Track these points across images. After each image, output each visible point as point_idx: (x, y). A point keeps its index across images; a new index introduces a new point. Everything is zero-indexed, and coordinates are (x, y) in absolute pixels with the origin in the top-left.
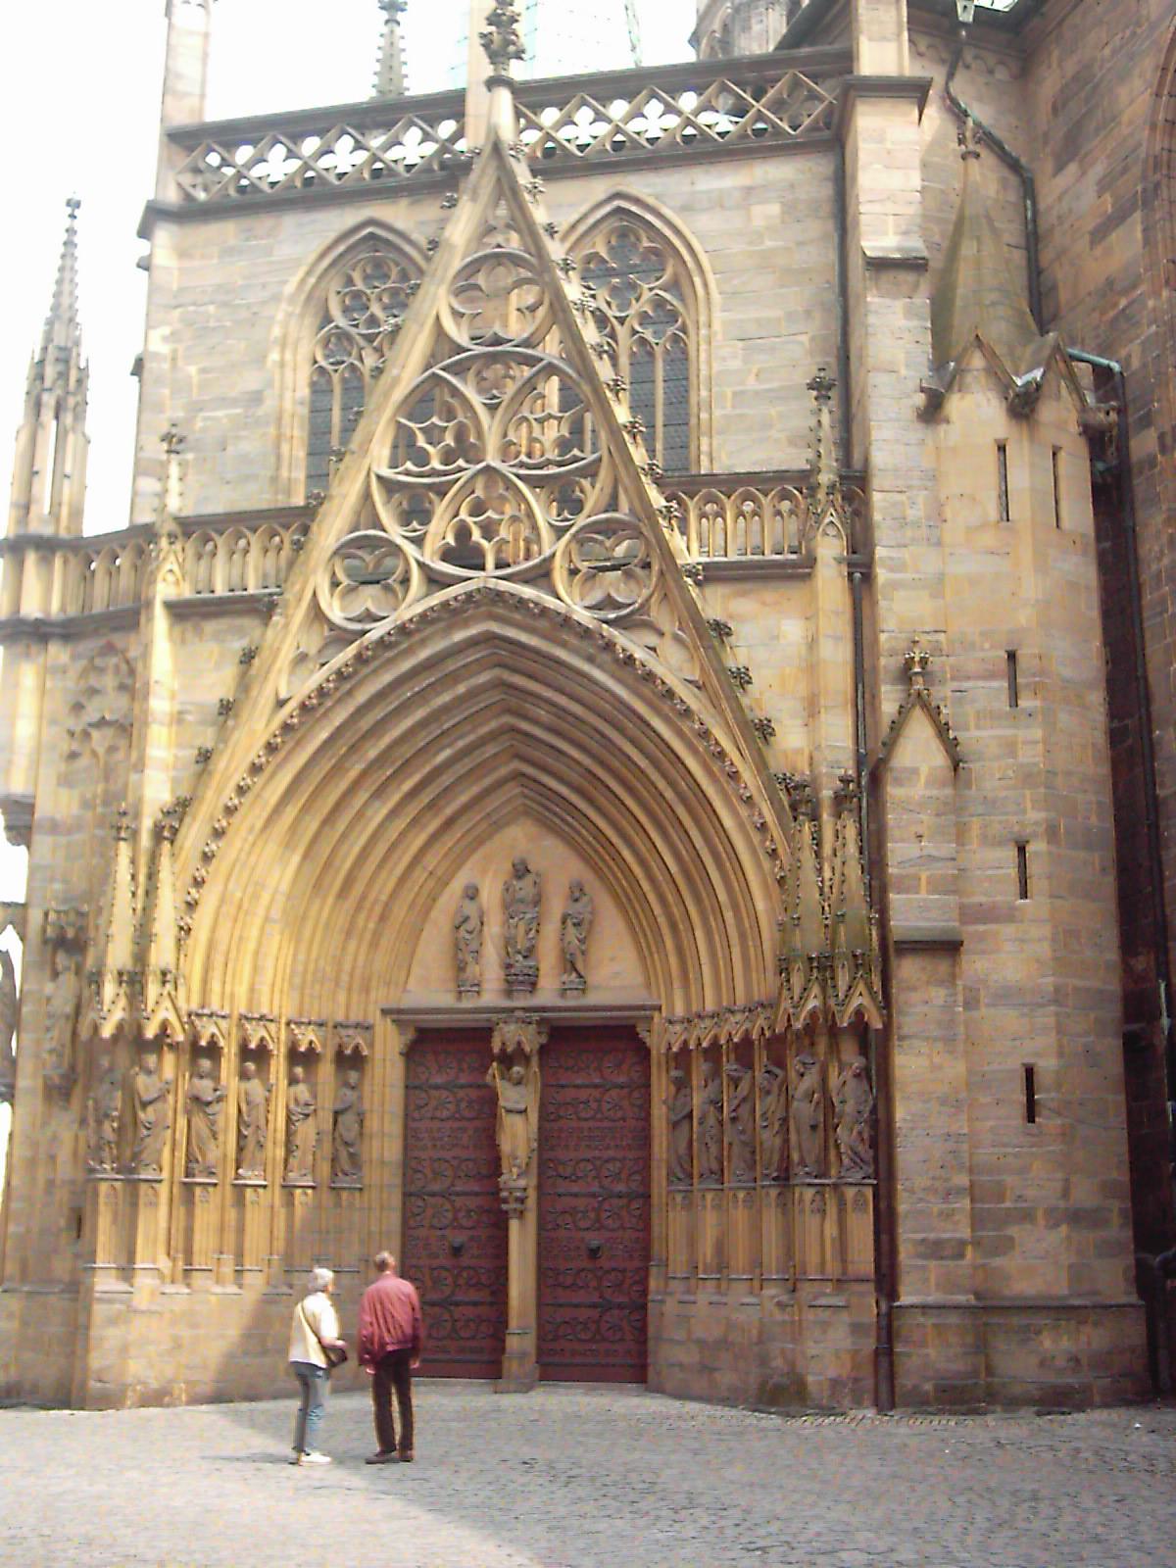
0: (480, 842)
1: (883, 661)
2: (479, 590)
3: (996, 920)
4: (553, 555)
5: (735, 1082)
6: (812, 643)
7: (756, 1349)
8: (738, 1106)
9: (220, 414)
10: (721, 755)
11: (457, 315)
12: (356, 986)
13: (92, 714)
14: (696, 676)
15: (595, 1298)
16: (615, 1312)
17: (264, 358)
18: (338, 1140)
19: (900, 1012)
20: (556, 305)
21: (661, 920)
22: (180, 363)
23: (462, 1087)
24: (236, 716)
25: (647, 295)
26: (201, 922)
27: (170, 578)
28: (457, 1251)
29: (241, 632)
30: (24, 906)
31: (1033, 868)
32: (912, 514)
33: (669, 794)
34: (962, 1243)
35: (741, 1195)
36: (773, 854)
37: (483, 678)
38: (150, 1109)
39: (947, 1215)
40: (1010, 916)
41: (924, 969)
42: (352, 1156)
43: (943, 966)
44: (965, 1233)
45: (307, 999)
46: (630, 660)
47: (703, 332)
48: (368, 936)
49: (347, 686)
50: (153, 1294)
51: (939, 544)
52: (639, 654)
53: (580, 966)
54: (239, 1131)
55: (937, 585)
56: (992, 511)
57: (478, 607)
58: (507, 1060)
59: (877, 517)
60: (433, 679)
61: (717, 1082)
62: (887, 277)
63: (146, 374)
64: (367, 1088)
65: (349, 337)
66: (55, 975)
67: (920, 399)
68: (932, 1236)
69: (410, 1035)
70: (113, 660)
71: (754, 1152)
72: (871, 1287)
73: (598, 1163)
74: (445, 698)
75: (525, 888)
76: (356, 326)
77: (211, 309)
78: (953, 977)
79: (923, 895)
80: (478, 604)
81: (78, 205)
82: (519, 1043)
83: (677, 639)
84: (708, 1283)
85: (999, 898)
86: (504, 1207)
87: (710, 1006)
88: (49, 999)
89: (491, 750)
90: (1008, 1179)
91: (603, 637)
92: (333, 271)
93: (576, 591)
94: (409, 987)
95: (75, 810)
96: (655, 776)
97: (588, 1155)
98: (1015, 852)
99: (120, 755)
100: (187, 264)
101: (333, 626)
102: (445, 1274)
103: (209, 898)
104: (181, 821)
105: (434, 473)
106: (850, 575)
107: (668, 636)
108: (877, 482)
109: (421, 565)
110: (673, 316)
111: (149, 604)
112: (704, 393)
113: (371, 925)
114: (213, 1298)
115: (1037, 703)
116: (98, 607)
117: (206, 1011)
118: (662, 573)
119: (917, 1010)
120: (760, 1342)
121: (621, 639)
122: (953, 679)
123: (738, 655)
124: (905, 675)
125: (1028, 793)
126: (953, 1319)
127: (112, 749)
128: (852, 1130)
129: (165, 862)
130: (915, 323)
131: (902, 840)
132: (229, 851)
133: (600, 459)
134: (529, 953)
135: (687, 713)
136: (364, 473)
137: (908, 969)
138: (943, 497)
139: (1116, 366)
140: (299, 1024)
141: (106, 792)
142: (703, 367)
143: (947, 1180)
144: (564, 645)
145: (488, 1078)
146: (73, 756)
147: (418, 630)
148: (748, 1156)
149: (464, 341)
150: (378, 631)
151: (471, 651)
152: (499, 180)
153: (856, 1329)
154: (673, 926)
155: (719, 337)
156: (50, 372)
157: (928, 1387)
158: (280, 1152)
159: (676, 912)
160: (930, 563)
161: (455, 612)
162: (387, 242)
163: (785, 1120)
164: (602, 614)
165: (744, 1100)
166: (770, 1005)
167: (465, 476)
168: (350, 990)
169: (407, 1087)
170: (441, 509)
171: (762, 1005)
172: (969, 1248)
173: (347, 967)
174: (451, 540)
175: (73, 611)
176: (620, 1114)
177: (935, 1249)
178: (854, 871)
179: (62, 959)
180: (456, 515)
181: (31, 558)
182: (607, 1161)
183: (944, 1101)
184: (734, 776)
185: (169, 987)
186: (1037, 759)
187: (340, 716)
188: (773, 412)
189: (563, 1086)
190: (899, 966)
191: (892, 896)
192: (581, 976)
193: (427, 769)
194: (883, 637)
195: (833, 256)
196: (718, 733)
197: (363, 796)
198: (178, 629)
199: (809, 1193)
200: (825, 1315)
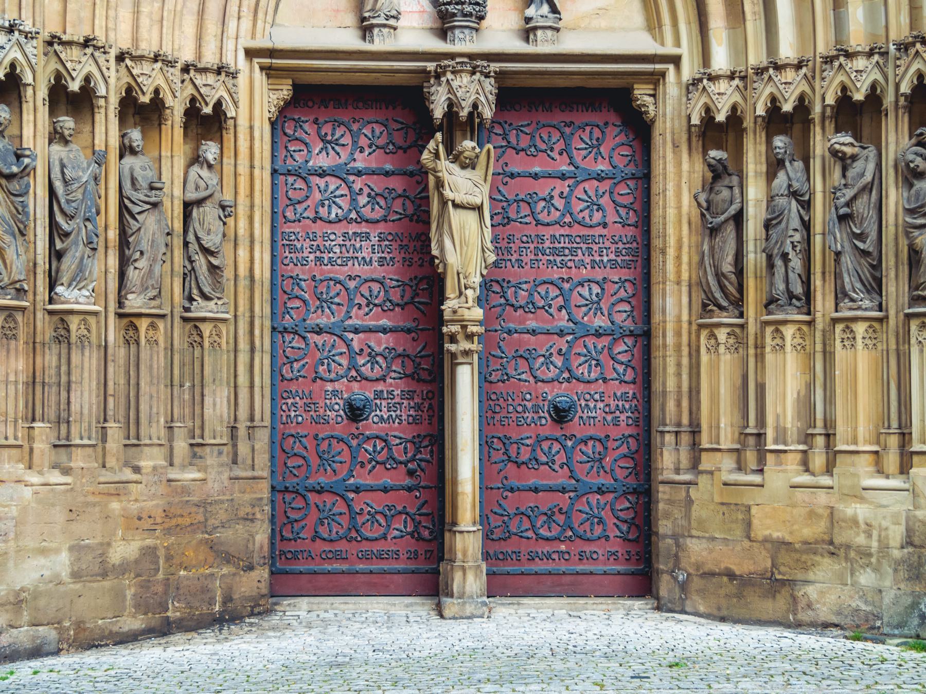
8: (854, 198)
18: (194, 247)
42: (214, 269)
45: (145, 21)
54: (53, 224)
69: (285, 91)
73: (566, 286)
84: (790, 456)
87: (787, 50)
97: (555, 274)
102: (338, 447)
114: (28, 492)
140: (133, 58)
145: (425, 155)
148: (866, 274)
158: (113, 261)
169: (274, 172)
176: (597, 217)
192: (554, 10)
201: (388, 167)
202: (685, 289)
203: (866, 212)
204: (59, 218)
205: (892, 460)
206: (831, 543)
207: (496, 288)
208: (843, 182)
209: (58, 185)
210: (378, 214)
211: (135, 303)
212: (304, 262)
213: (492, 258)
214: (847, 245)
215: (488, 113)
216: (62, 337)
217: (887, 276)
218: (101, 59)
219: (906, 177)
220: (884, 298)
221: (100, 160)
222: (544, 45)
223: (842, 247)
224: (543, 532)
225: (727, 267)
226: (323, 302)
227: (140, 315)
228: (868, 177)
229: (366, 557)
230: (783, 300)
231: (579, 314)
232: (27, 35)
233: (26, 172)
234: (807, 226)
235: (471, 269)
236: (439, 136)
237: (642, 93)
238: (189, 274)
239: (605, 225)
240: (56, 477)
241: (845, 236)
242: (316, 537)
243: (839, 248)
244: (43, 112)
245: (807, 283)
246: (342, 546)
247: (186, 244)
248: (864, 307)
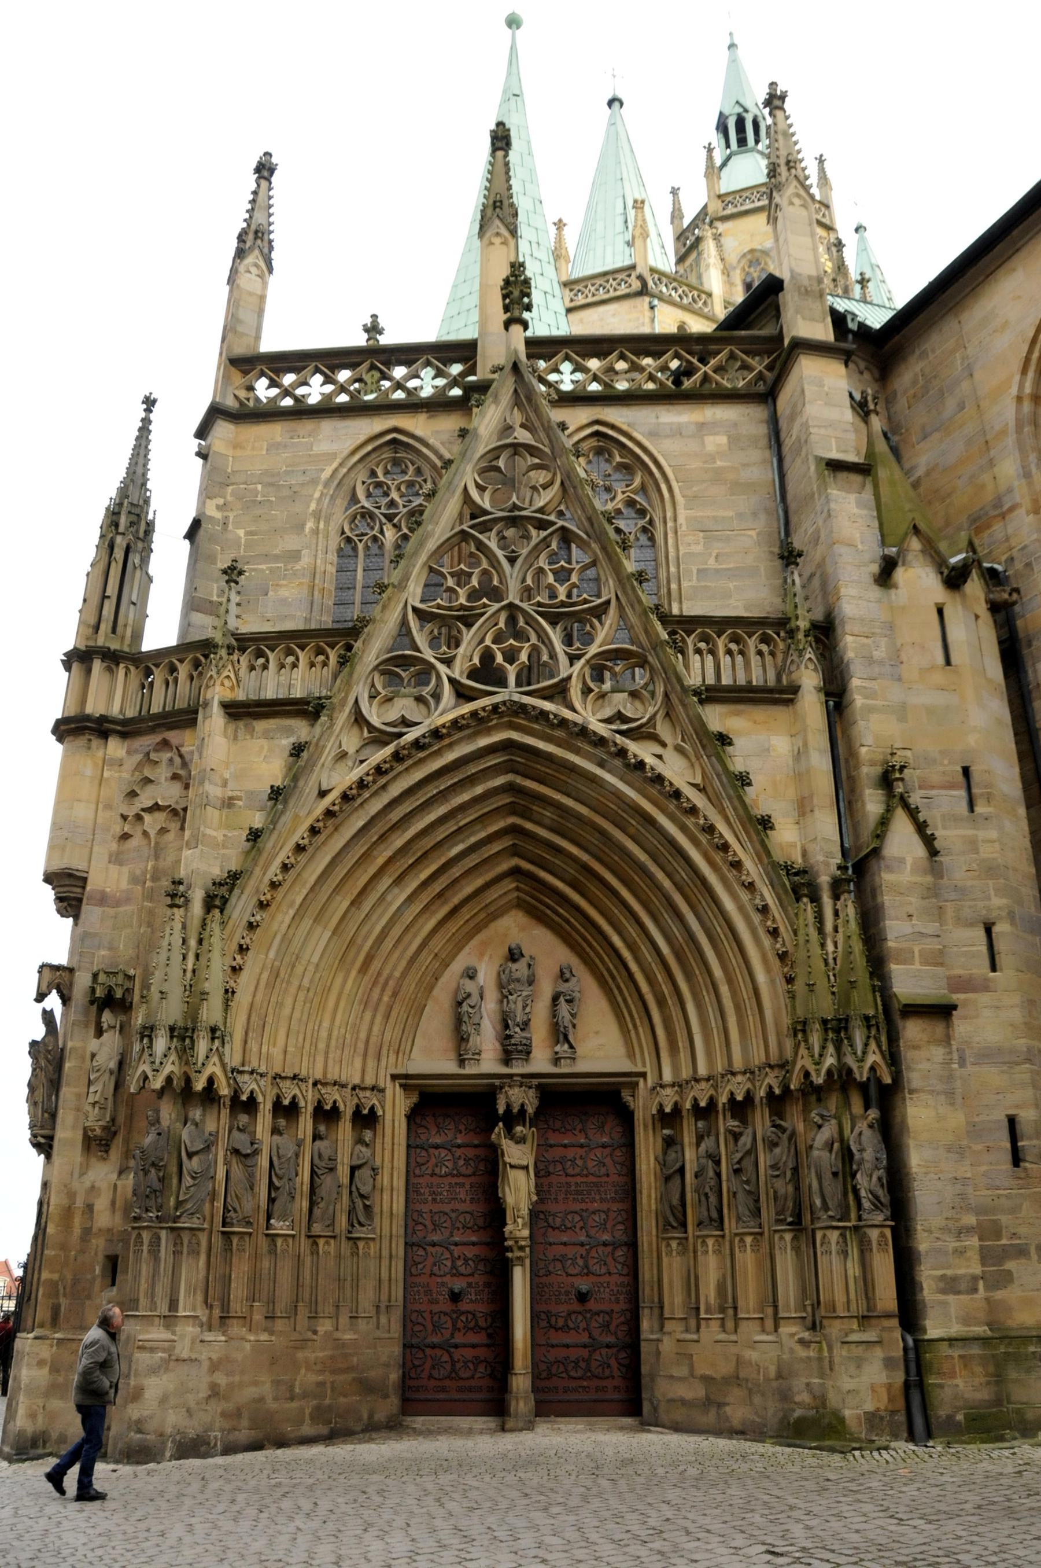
0: (478, 929)
1: (865, 770)
2: (504, 703)
3: (974, 990)
4: (570, 677)
5: (736, 1136)
6: (799, 755)
7: (775, 1384)
8: (741, 1159)
9: (263, 567)
10: (725, 847)
11: (481, 489)
12: (372, 1050)
13: (145, 799)
14: (698, 780)
15: (585, 1339)
16: (604, 1351)
17: (302, 526)
18: (355, 1194)
19: (909, 1068)
20: (567, 483)
21: (650, 998)
22: (230, 527)
23: (459, 1146)
24: (286, 802)
25: (620, 497)
26: (245, 983)
27: (227, 683)
28: (455, 1297)
29: (289, 731)
30: (70, 970)
31: (1000, 946)
32: (877, 654)
33: (667, 884)
34: (975, 1279)
35: (749, 1240)
36: (774, 933)
37: (499, 781)
38: (195, 1160)
39: (960, 1252)
40: (985, 987)
41: (924, 1030)
42: (367, 1208)
43: (939, 1028)
44: (977, 1269)
45: (330, 1063)
46: (641, 765)
47: (670, 524)
48: (382, 1009)
49: (383, 781)
50: (193, 1342)
51: (900, 679)
52: (650, 760)
53: (571, 1038)
54: (271, 1183)
55: (901, 712)
56: (940, 659)
57: (501, 717)
58: (512, 1119)
59: (850, 654)
60: (456, 780)
61: (713, 1138)
62: (843, 476)
63: (201, 533)
64: (378, 1146)
65: (372, 516)
66: (99, 1032)
67: (875, 568)
68: (949, 1272)
69: (415, 1099)
70: (166, 756)
71: (757, 1201)
72: (895, 1322)
73: (585, 1214)
74: (465, 797)
75: (520, 969)
76: (379, 508)
77: (259, 487)
78: (947, 1040)
79: (917, 966)
80: (502, 715)
81: (154, 401)
82: (522, 1105)
83: (679, 749)
84: (712, 1323)
85: (974, 971)
86: (509, 1255)
87: (702, 1070)
88: (93, 1056)
89: (496, 847)
90: (1004, 1219)
91: (616, 744)
92: (360, 466)
93: (589, 707)
94: (413, 1056)
95: (124, 885)
96: (653, 868)
97: (577, 1207)
98: (981, 933)
99: (170, 836)
100: (239, 453)
101: (371, 728)
102: (444, 1319)
103: (252, 965)
104: (231, 891)
105: (462, 607)
106: (827, 702)
107: (670, 747)
108: (848, 628)
109: (451, 680)
110: (642, 512)
111: (206, 704)
112: (673, 569)
113: (386, 999)
114: (248, 1346)
115: (990, 809)
116: (155, 709)
117: (246, 1068)
118: (666, 695)
119: (920, 1066)
120: (779, 1376)
121: (635, 748)
122: (920, 788)
123: (739, 759)
124: (887, 780)
125: (990, 882)
126: (975, 1350)
127: (163, 831)
128: (871, 1176)
129: (215, 927)
130: (864, 512)
131: (897, 919)
132: (281, 919)
133: (608, 603)
134: (525, 1025)
135: (693, 811)
136: (401, 605)
137: (912, 1030)
138: (899, 644)
139: (996, 566)
141: (155, 869)
142: (671, 550)
143: (958, 1220)
144: (577, 751)
145: (493, 1136)
146: (125, 837)
147: (449, 735)
148: (752, 1206)
149: (487, 506)
150: (412, 735)
151: (491, 756)
152: (516, 391)
153: (889, 1363)
154: (661, 1002)
155: (684, 528)
156: (123, 521)
157: (960, 1417)
158: (305, 1204)
159: (666, 989)
160: (895, 694)
161: (481, 721)
162: (407, 446)
163: (795, 1170)
164: (614, 727)
165: (748, 1153)
166: (784, 1065)
167: (491, 611)
168: (365, 1055)
169: (408, 1146)
170: (468, 636)
171: (771, 1067)
172: (981, 1283)
173: (363, 1035)
174: (476, 660)
175: (131, 713)
176: (603, 1170)
177: (950, 1285)
178: (858, 946)
179: (107, 1017)
180: (482, 641)
181: (97, 665)
182: (594, 1213)
183: (949, 1149)
184: (737, 865)
185: (217, 1042)
186: (995, 855)
187: (376, 806)
188: (731, 585)
189: (551, 1146)
190: (904, 1028)
191: (893, 967)
192: (571, 1047)
193: (443, 860)
194: (863, 750)
195: (770, 474)
196: (721, 827)
197: (386, 881)
198: (232, 727)
199: (834, 1236)
200: (858, 1351)
201: (476, 1142)
202: (653, 1215)
204: (275, 1179)
205: (769, 1323)
206: (738, 1378)
207: (542, 1216)
209: (275, 1159)
210: (470, 1171)
211: (317, 1229)
212: (425, 1202)
213: (535, 1198)
215: (530, 1110)
216: (273, 1251)
218: (304, 1088)
221: (300, 1144)
222: (565, 1068)
224: (573, 1374)
225: (675, 1201)
226: (436, 1227)
227: (320, 1236)
228: (748, 1146)
229: (460, 1390)
230: (707, 1222)
231: (592, 1232)
232: (262, 1075)
233: (256, 1152)
234: (718, 1175)
235: (522, 1206)
236: (501, 1124)
237: (626, 1096)
238: (352, 1211)
239: (608, 1175)
240: (264, 1337)
242: (430, 1377)
244: (269, 1117)
245: (720, 1211)
246: (447, 1383)
247: (351, 1192)
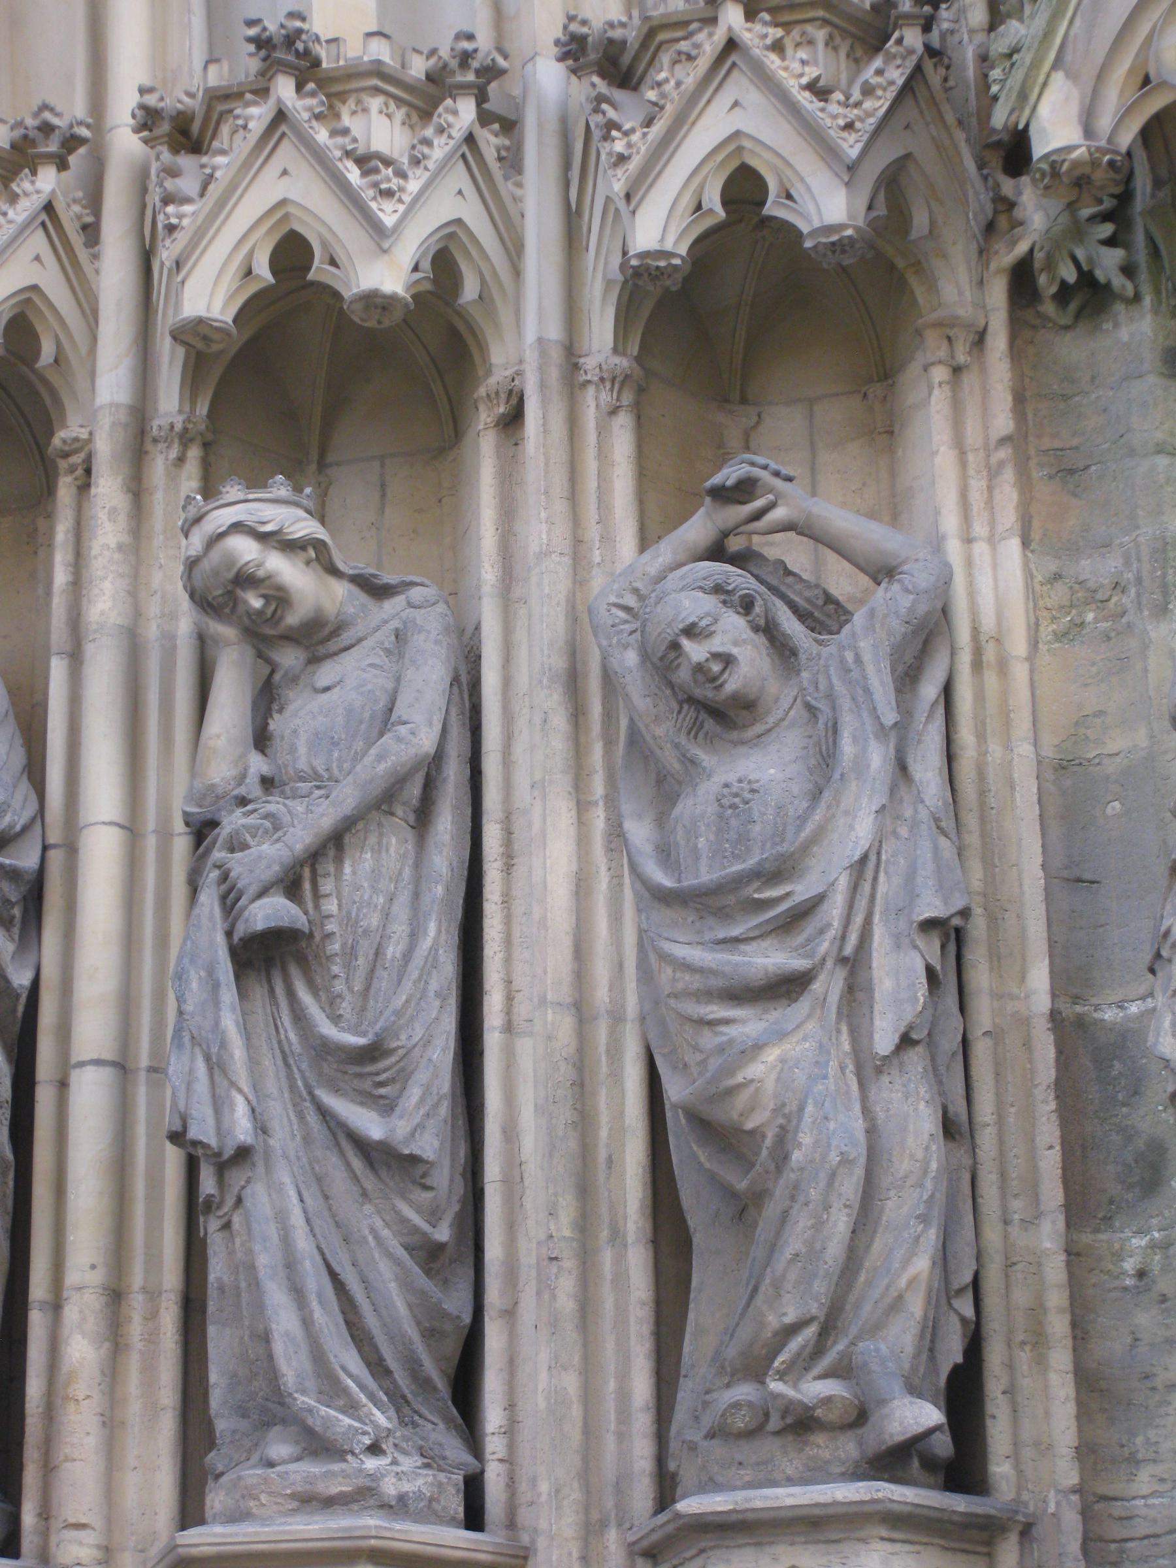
203: (400, 929)
208: (258, 764)
214: (279, 1112)
217: (510, 1314)
219: (635, 739)
220: (494, 1446)
223: (262, 1129)
241: (270, 1064)
243: (242, 1129)
248: (390, 1488)
